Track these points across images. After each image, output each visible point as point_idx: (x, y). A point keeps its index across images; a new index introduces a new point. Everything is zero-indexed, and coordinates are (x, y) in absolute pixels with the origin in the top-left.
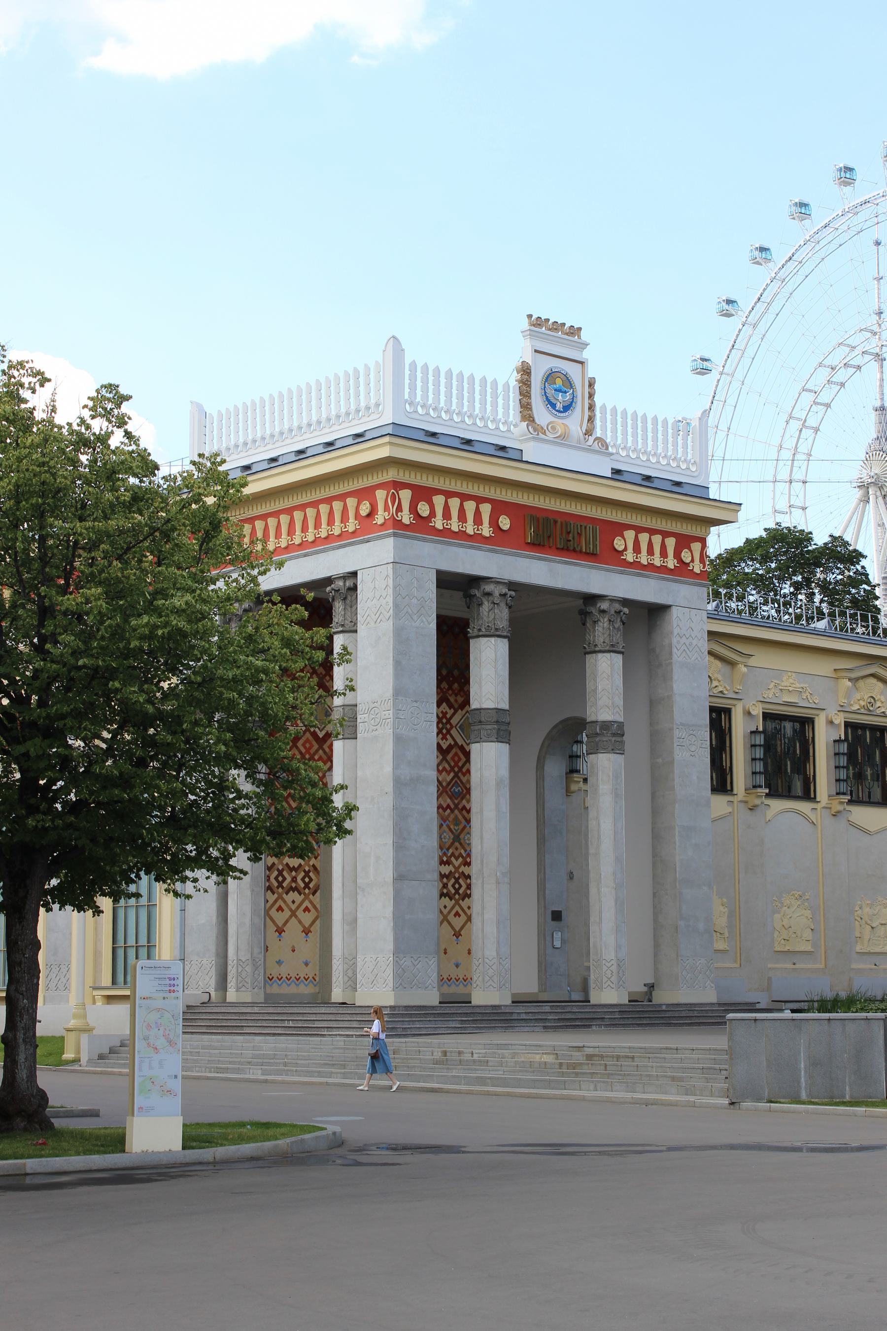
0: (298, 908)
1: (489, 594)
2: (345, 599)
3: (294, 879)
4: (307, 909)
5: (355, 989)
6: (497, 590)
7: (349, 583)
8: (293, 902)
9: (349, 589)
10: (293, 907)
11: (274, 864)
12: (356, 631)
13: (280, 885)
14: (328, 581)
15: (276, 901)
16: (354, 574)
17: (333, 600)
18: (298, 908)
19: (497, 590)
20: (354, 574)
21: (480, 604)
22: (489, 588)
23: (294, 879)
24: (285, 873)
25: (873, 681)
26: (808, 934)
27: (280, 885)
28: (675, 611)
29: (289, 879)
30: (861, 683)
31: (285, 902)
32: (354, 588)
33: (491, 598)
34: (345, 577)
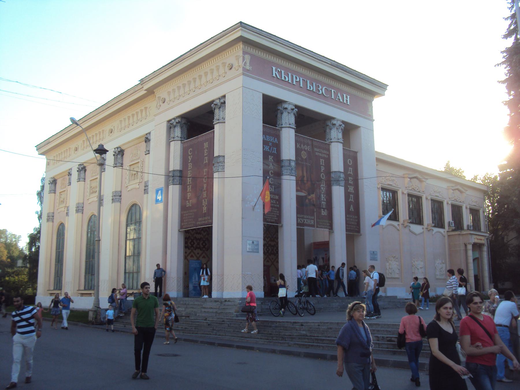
0: (200, 256)
1: (286, 108)
2: (220, 108)
3: (198, 244)
4: (204, 257)
5: (223, 290)
6: (290, 107)
7: (222, 101)
8: (198, 253)
9: (222, 103)
10: (198, 256)
11: (189, 237)
12: (225, 122)
13: (192, 246)
14: (212, 102)
15: (190, 253)
16: (224, 96)
17: (215, 109)
18: (200, 256)
19: (290, 107)
20: (224, 96)
21: (282, 113)
22: (286, 106)
23: (198, 244)
24: (194, 241)
25: (415, 180)
26: (397, 271)
27: (192, 246)
28: (362, 129)
29: (196, 243)
30: (413, 180)
31: (194, 253)
32: (224, 103)
33: (287, 110)
34: (219, 99)
